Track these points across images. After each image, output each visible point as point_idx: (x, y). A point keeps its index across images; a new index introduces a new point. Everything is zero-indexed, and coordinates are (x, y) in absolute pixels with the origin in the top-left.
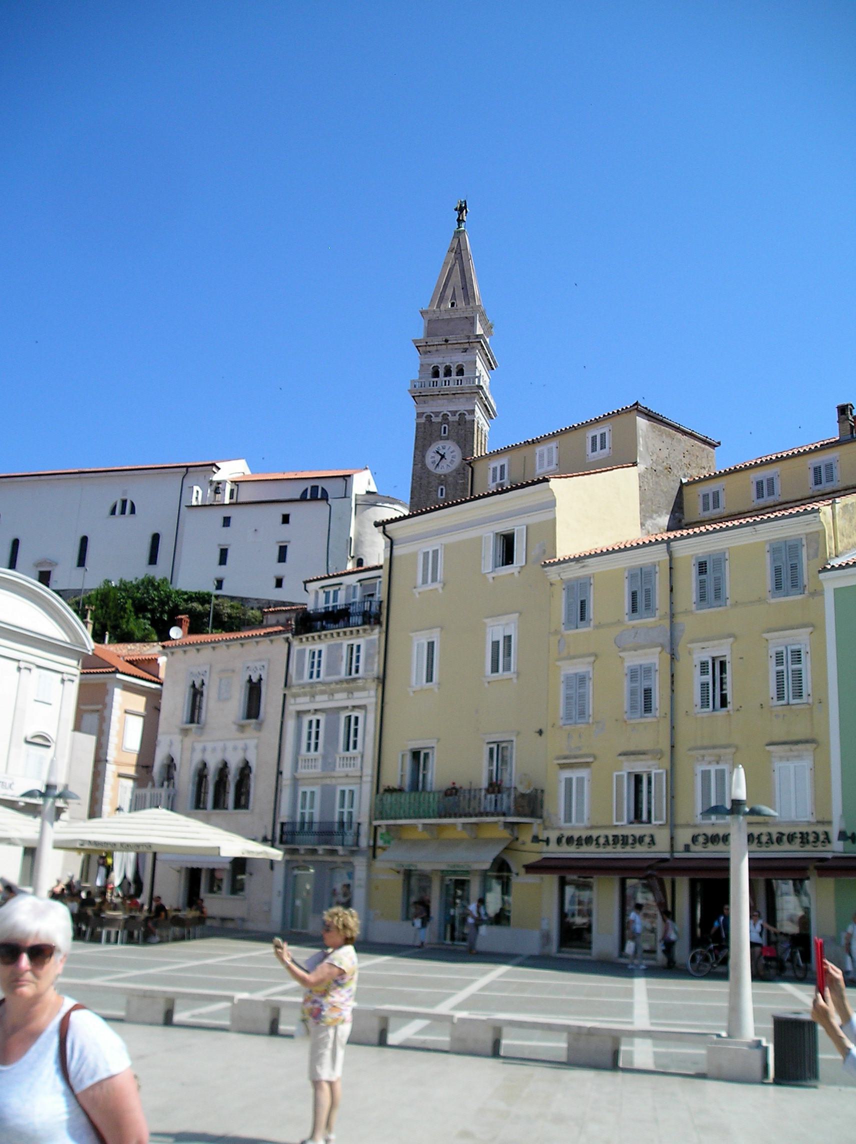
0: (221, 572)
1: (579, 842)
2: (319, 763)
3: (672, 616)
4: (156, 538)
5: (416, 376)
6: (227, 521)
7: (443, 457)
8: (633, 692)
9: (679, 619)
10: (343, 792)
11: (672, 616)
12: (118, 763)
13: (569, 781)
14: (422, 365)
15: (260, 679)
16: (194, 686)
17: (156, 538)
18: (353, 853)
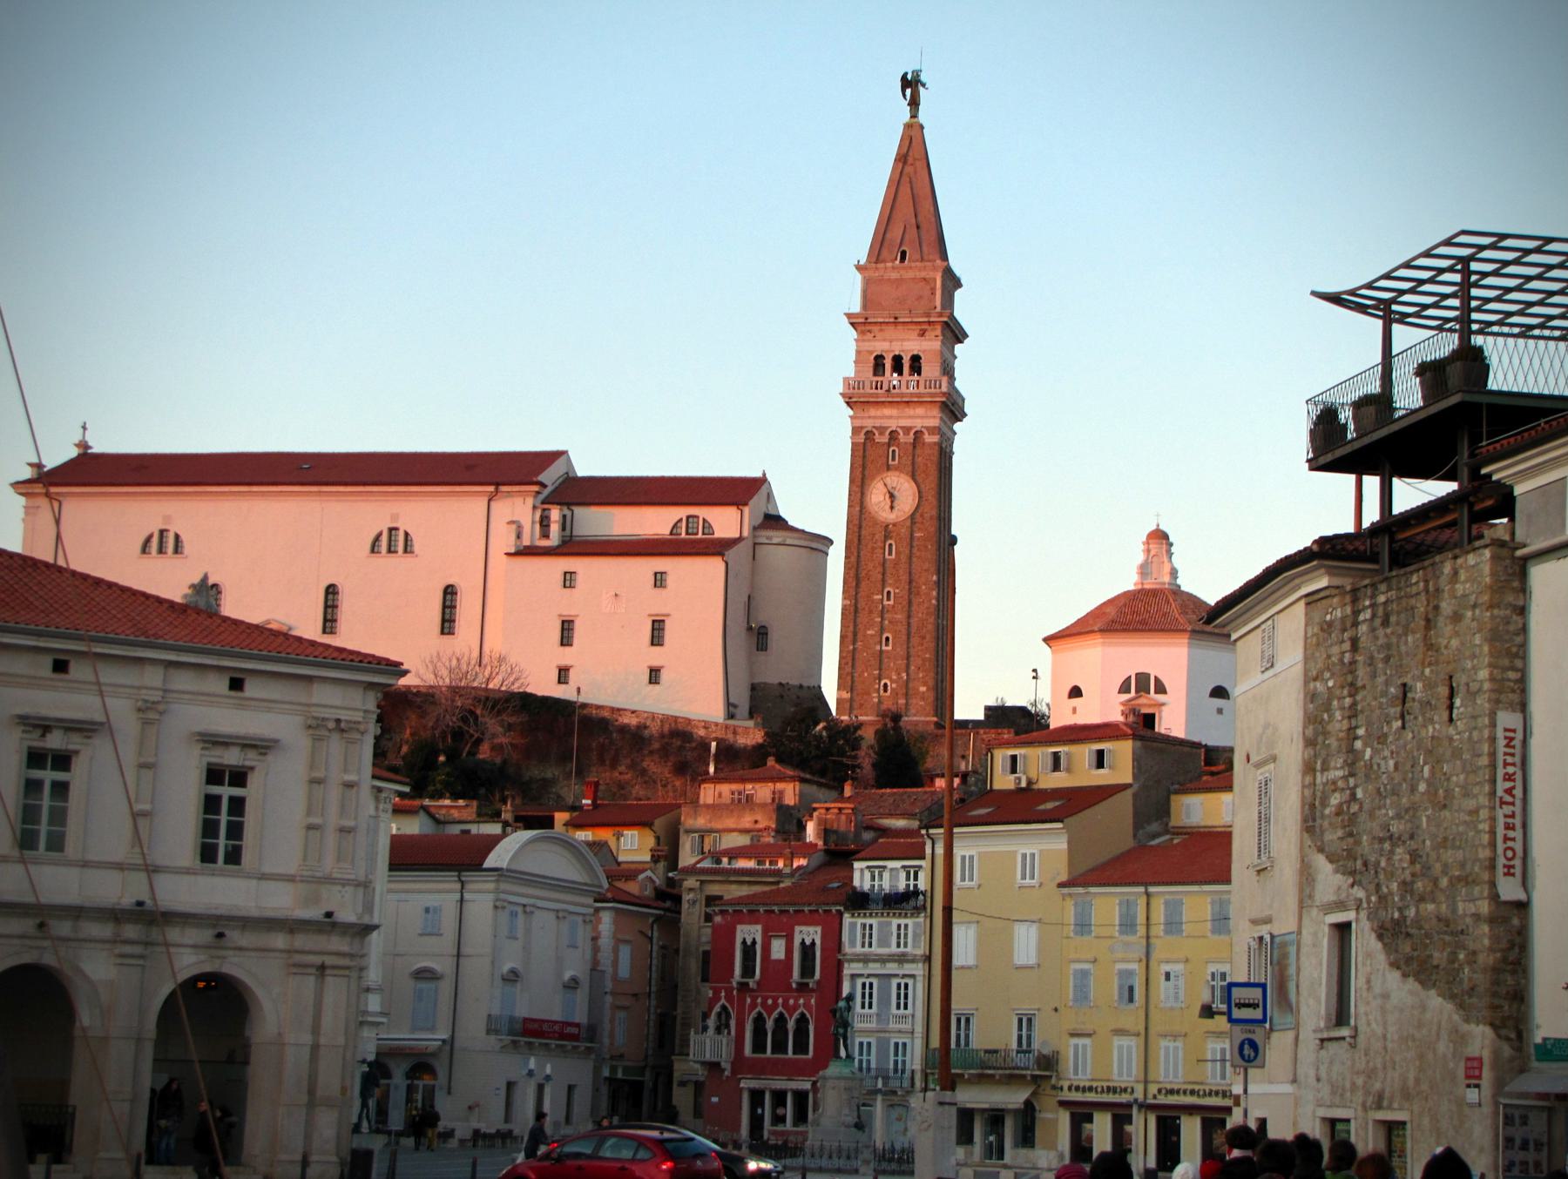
0: (566, 656)
1: (1084, 1090)
3: (1148, 937)
4: (450, 592)
5: (850, 371)
6: (569, 580)
7: (892, 496)
8: (1121, 987)
9: (1152, 941)
10: (897, 1045)
11: (1148, 937)
12: (613, 993)
13: (1076, 1047)
14: (858, 352)
16: (744, 942)
17: (450, 592)
18: (908, 1093)
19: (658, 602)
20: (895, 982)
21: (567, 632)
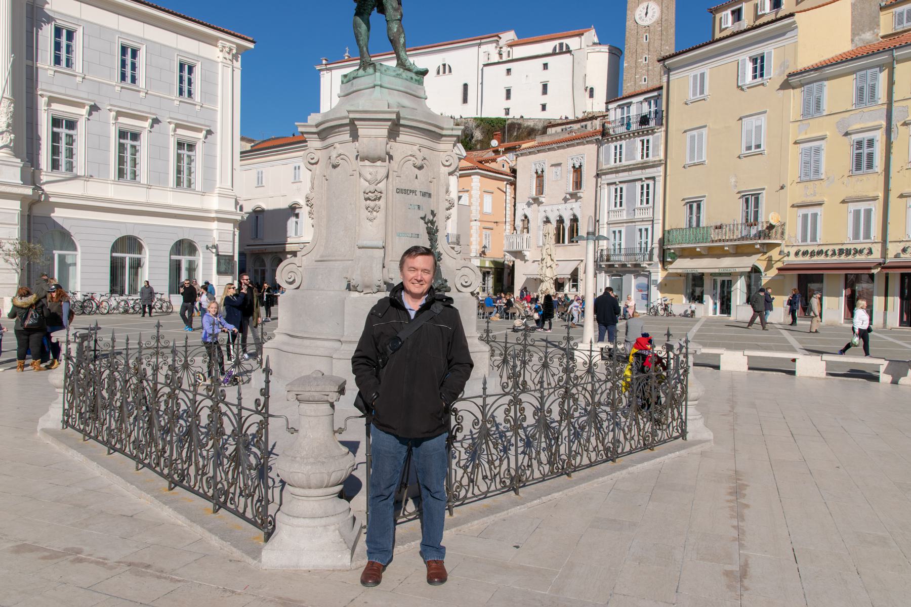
0: (508, 104)
1: (812, 254)
2: (625, 212)
6: (509, 71)
15: (580, 166)
16: (537, 173)
19: (545, 76)
20: (638, 185)
21: (508, 92)
